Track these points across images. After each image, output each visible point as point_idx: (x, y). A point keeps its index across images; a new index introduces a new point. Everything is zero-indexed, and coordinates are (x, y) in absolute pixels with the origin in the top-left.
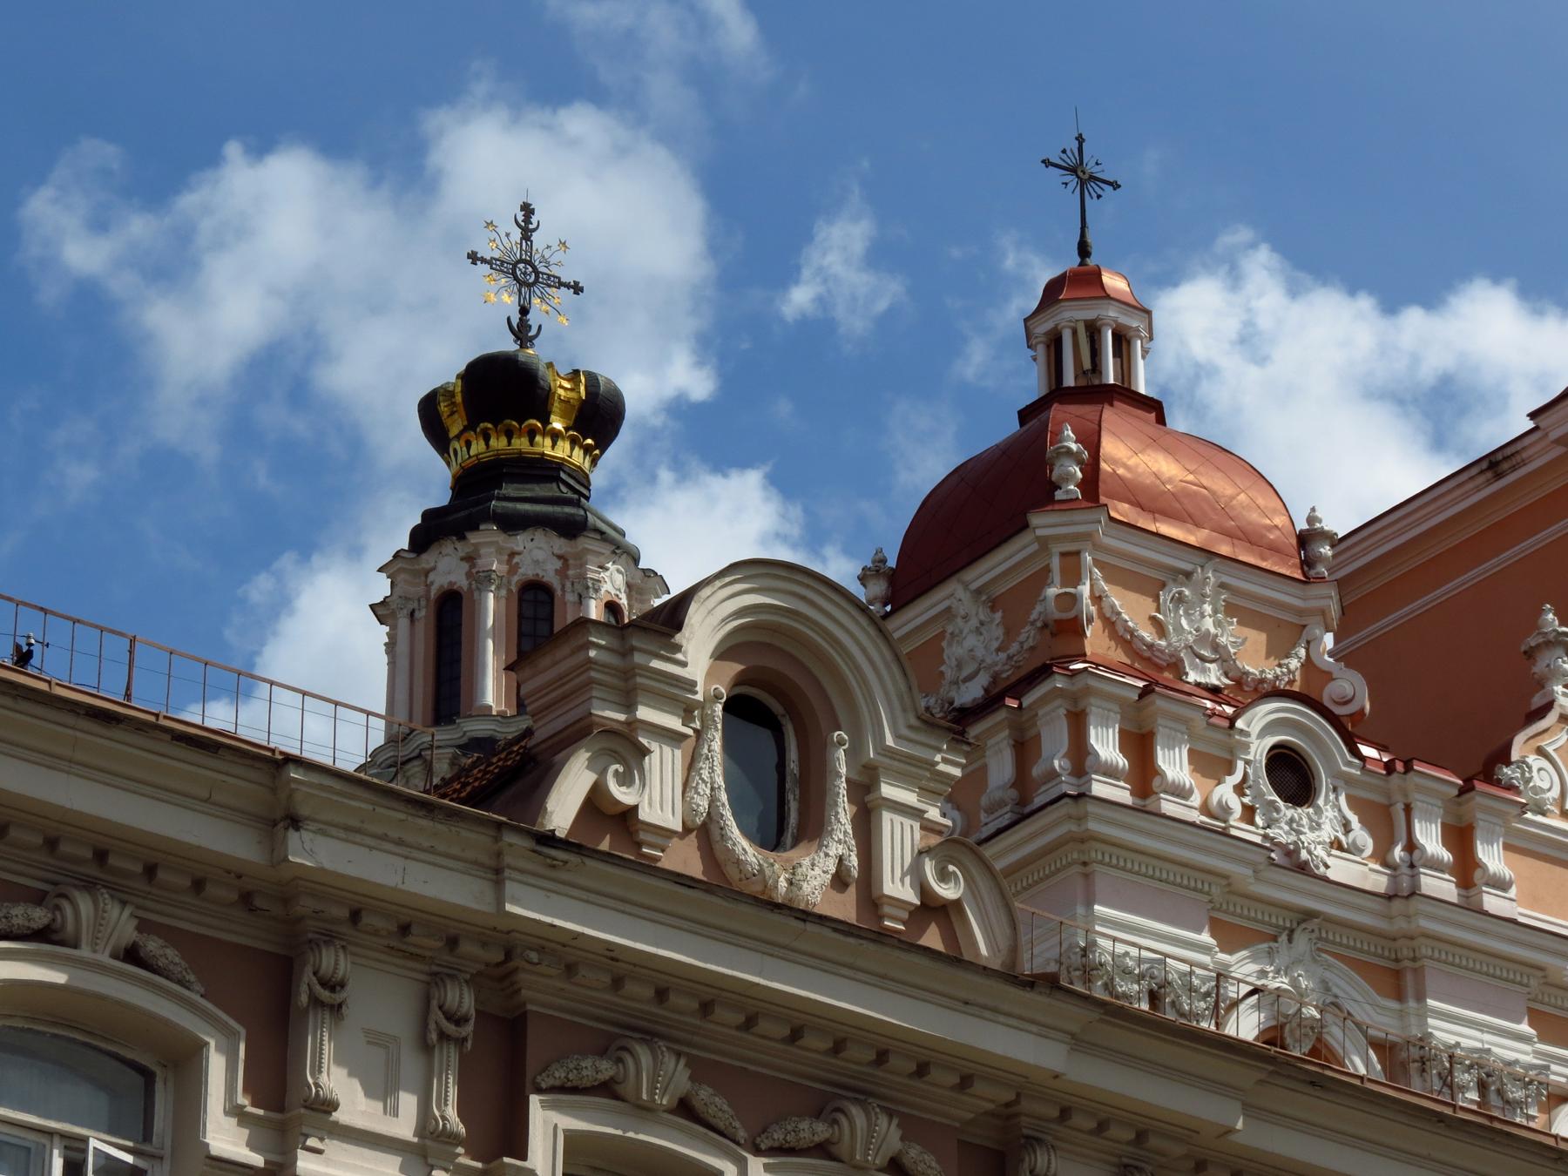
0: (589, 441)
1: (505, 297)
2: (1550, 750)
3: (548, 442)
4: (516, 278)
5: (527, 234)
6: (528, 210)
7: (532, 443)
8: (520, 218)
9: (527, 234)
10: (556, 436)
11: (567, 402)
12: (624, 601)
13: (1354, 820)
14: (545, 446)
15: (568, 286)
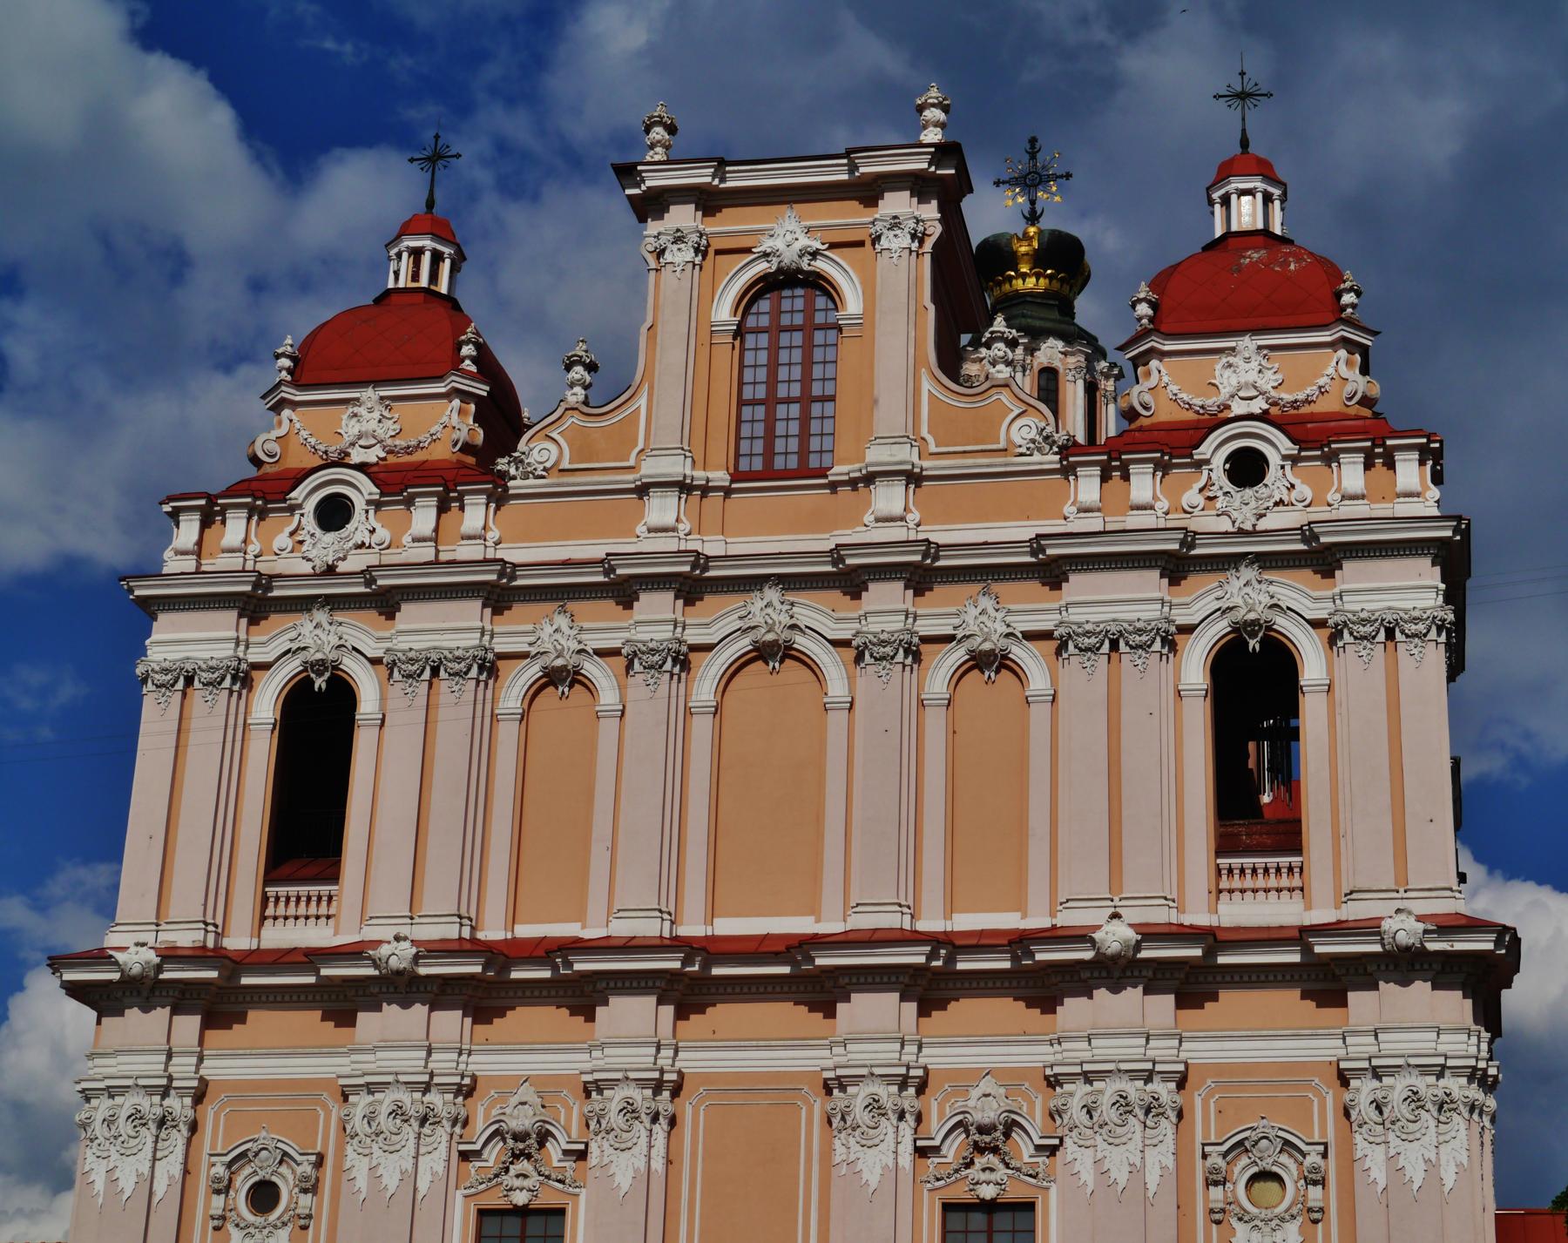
0: (1049, 272)
1: (1020, 200)
2: (554, 435)
3: (1020, 281)
4: (1027, 185)
5: (1033, 156)
6: (1033, 141)
7: (1011, 286)
8: (1028, 146)
9: (1033, 156)
10: (1024, 276)
11: (1027, 254)
12: (1057, 364)
13: (378, 526)
14: (1019, 284)
15: (1061, 177)
